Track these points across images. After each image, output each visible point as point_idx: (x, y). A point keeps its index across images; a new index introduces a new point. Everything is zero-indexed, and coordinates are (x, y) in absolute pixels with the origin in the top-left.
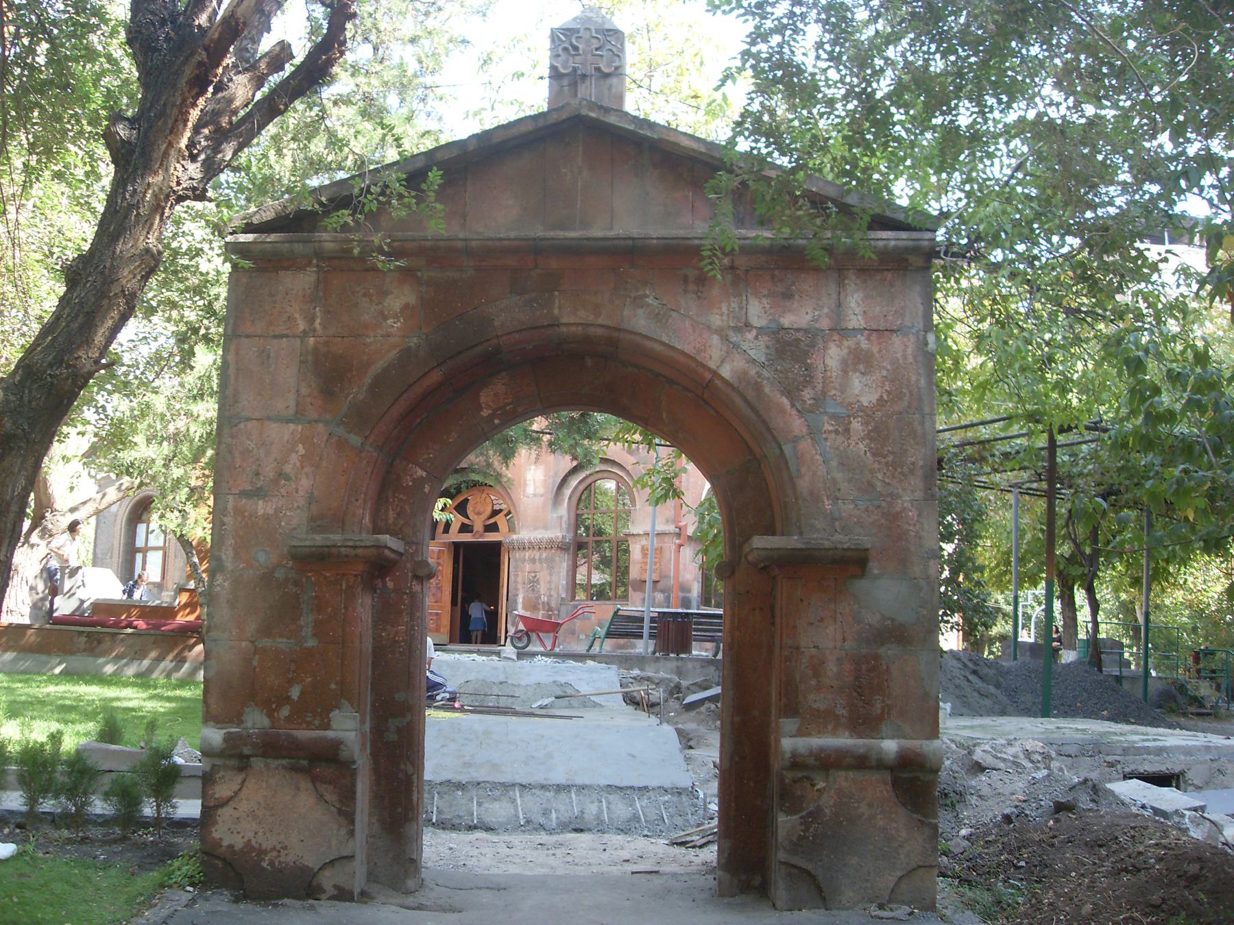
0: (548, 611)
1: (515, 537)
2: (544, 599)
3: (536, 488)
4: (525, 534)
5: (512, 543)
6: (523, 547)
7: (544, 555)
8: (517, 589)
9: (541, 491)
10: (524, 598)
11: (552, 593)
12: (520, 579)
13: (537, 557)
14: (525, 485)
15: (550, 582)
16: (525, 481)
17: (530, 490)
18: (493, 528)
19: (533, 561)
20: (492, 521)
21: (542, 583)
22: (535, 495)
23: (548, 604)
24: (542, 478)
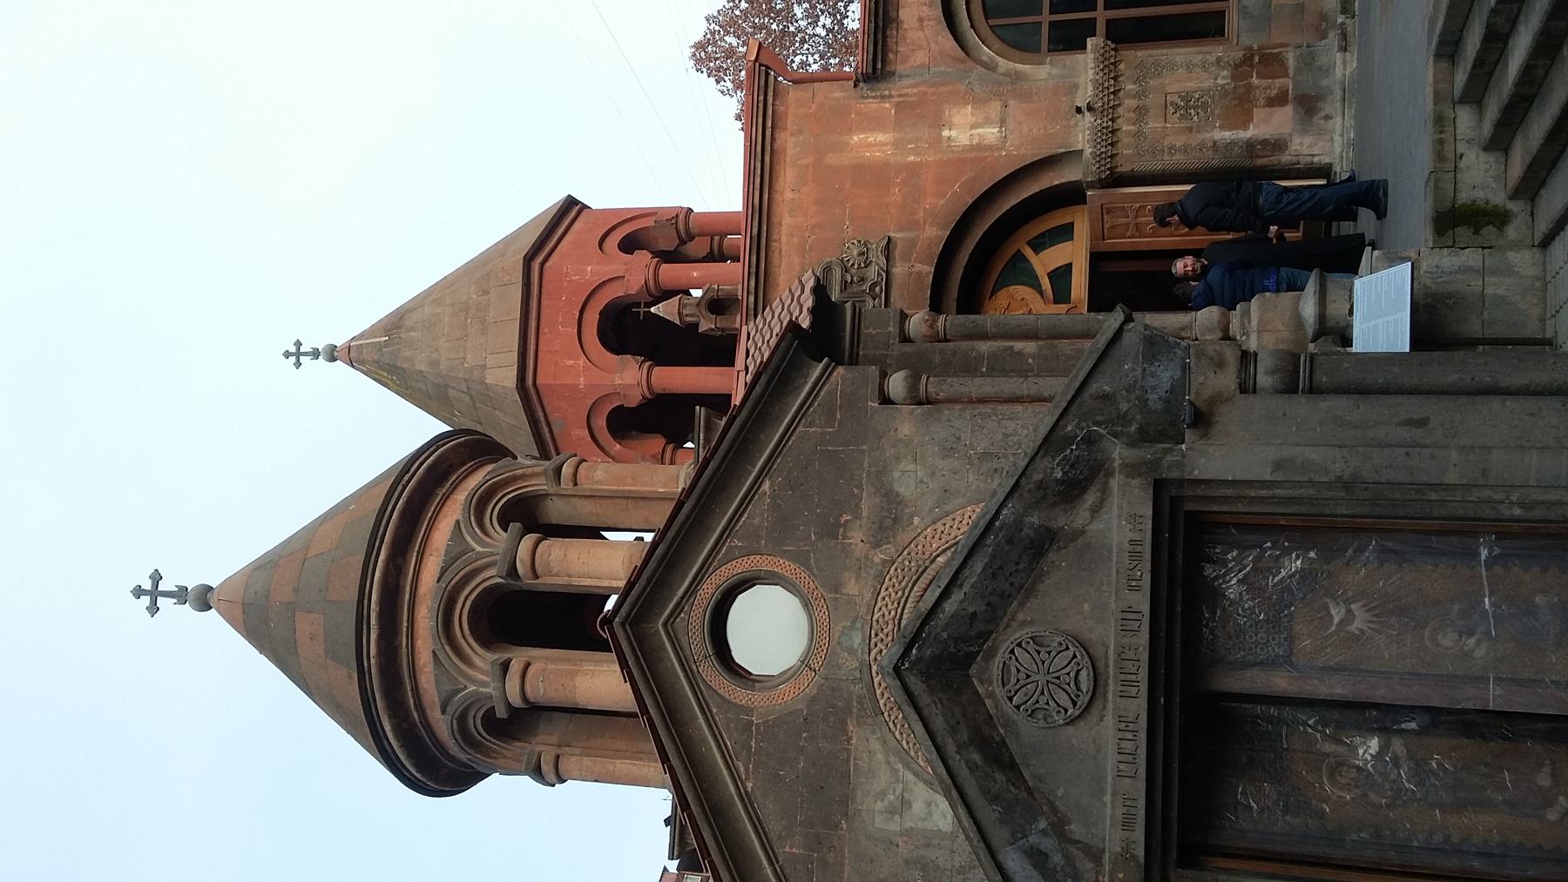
0: (1252, 66)
1: (1088, 151)
2: (1224, 78)
3: (987, 122)
4: (1083, 136)
5: (1099, 157)
6: (1109, 136)
7: (1130, 87)
8: (1202, 146)
9: (995, 107)
10: (1222, 127)
11: (1212, 59)
12: (1179, 141)
13: (1132, 103)
14: (979, 147)
15: (1189, 67)
16: (973, 148)
17: (991, 133)
18: (1061, 276)
19: (1141, 112)
20: (1046, 284)
21: (1191, 85)
22: (1003, 122)
23: (1236, 67)
24: (969, 108)
